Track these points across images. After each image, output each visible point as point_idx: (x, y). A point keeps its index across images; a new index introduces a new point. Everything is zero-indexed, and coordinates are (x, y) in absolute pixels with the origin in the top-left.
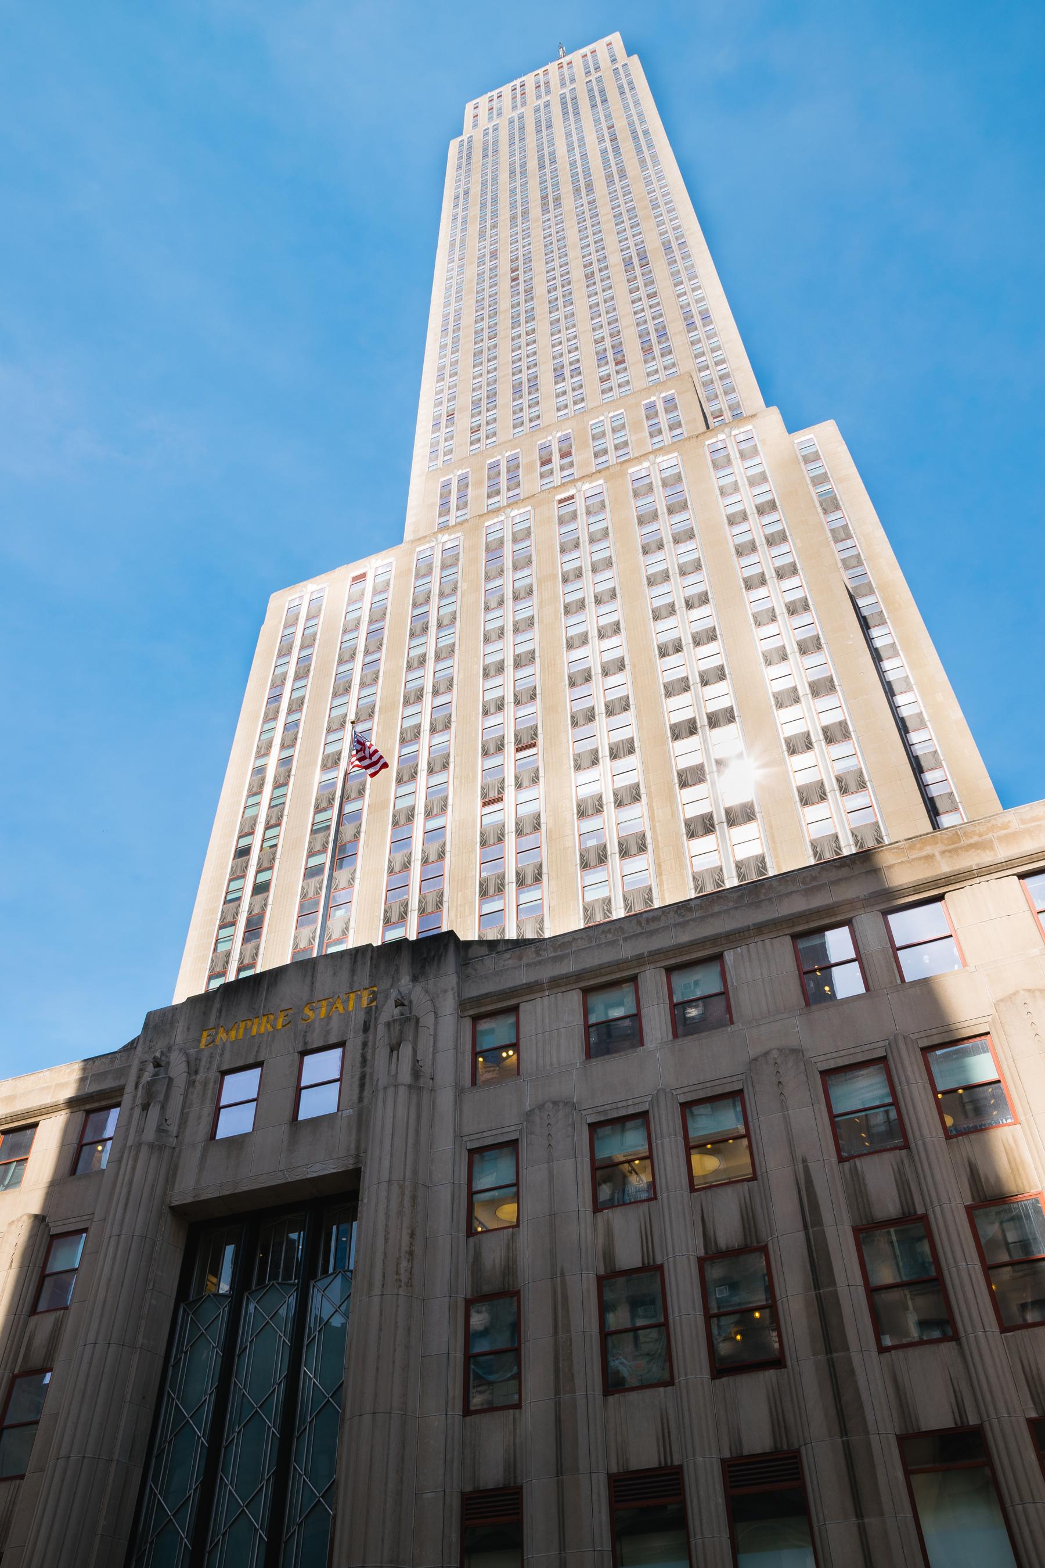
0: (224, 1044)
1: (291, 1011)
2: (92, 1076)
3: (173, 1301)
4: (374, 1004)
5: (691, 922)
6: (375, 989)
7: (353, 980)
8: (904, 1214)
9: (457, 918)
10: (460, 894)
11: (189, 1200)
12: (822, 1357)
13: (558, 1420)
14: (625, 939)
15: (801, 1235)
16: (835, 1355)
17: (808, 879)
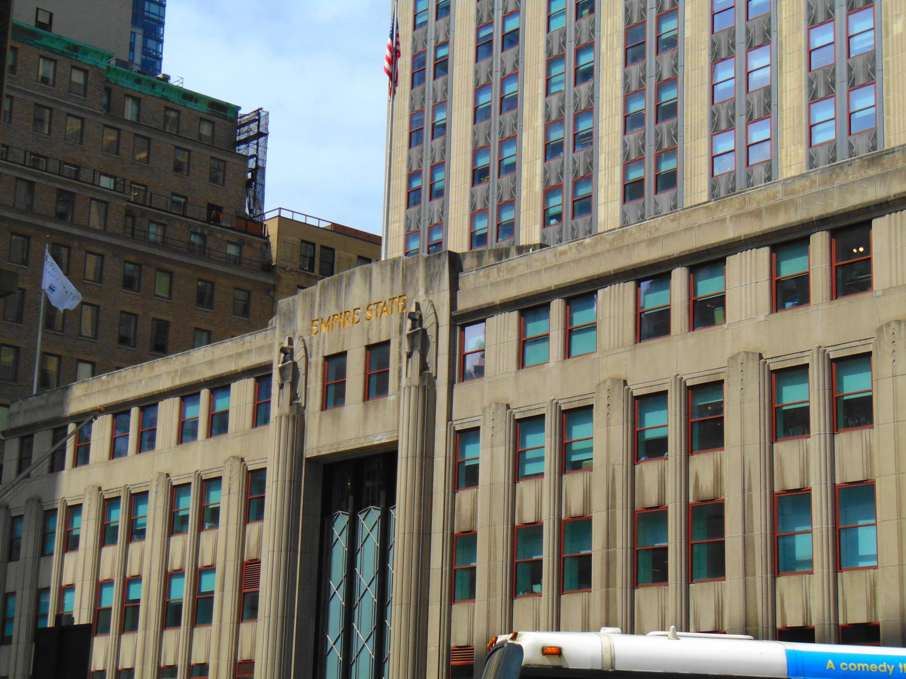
0: (324, 334)
1: (359, 311)
2: (256, 348)
3: (319, 518)
4: (405, 311)
5: (583, 260)
6: (405, 298)
7: (393, 288)
8: (659, 504)
9: (607, 52)
10: (609, 20)
11: (315, 454)
12: (604, 590)
13: (488, 612)
14: (546, 269)
15: (605, 513)
16: (610, 589)
17: (653, 229)
